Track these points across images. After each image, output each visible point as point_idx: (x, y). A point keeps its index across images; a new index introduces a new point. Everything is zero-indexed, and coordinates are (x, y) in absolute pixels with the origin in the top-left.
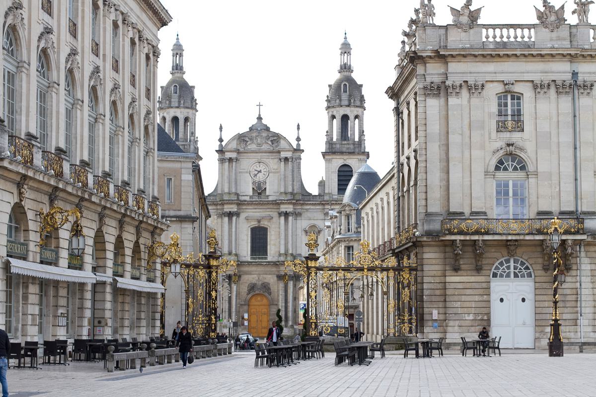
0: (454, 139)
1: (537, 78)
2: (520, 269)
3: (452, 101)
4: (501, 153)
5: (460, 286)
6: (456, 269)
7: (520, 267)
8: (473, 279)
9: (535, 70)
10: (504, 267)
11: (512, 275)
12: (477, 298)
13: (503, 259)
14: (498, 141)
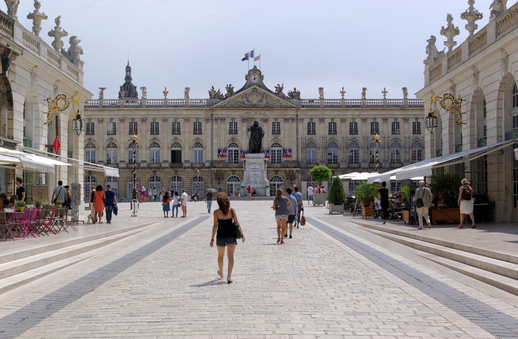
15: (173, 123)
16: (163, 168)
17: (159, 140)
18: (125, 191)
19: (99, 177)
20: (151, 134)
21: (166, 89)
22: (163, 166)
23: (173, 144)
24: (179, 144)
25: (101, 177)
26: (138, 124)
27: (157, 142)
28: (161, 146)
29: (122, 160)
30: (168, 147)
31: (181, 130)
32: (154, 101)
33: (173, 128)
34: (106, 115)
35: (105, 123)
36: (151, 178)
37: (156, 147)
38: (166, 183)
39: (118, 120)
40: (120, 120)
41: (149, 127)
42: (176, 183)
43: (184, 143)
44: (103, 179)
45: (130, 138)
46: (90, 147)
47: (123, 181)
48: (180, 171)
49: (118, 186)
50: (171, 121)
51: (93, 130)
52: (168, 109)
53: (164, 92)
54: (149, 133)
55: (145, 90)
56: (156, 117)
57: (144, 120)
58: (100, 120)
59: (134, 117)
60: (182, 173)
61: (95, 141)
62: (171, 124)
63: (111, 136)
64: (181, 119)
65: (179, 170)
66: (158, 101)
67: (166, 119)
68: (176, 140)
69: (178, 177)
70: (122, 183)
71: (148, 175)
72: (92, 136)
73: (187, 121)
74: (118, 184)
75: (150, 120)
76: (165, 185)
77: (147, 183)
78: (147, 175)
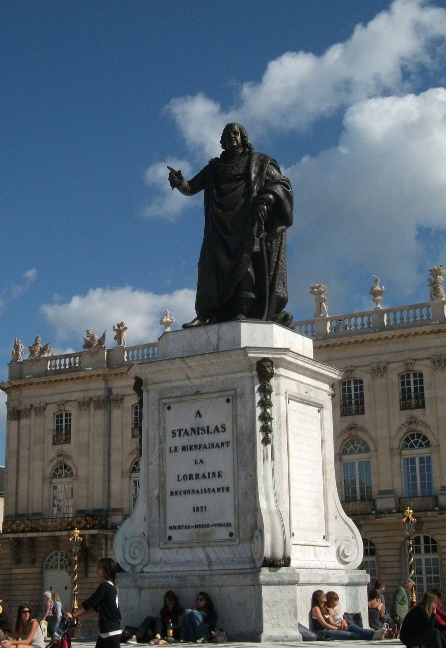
0: (24, 453)
1: (78, 396)
2: (65, 561)
3: (24, 422)
4: (55, 462)
5: (20, 577)
6: (18, 562)
7: (64, 559)
8: (29, 571)
9: (75, 391)
10: (54, 559)
11: (59, 566)
12: (31, 587)
13: (53, 553)
14: (52, 452)
15: (403, 377)
16: (380, 513)
17: (364, 430)
22: (378, 508)
23: (407, 440)
24: (425, 438)
27: (360, 434)
28: (372, 447)
30: (391, 450)
31: (427, 394)
33: (403, 390)
38: (391, 559)
42: (423, 557)
43: (435, 432)
48: (430, 522)
50: (396, 369)
52: (383, 337)
56: (355, 362)
60: (434, 525)
62: (396, 379)
64: (424, 362)
65: (426, 516)
66: (359, 320)
67: (382, 364)
68: (413, 426)
69: (427, 539)
73: (440, 365)
76: (388, 565)
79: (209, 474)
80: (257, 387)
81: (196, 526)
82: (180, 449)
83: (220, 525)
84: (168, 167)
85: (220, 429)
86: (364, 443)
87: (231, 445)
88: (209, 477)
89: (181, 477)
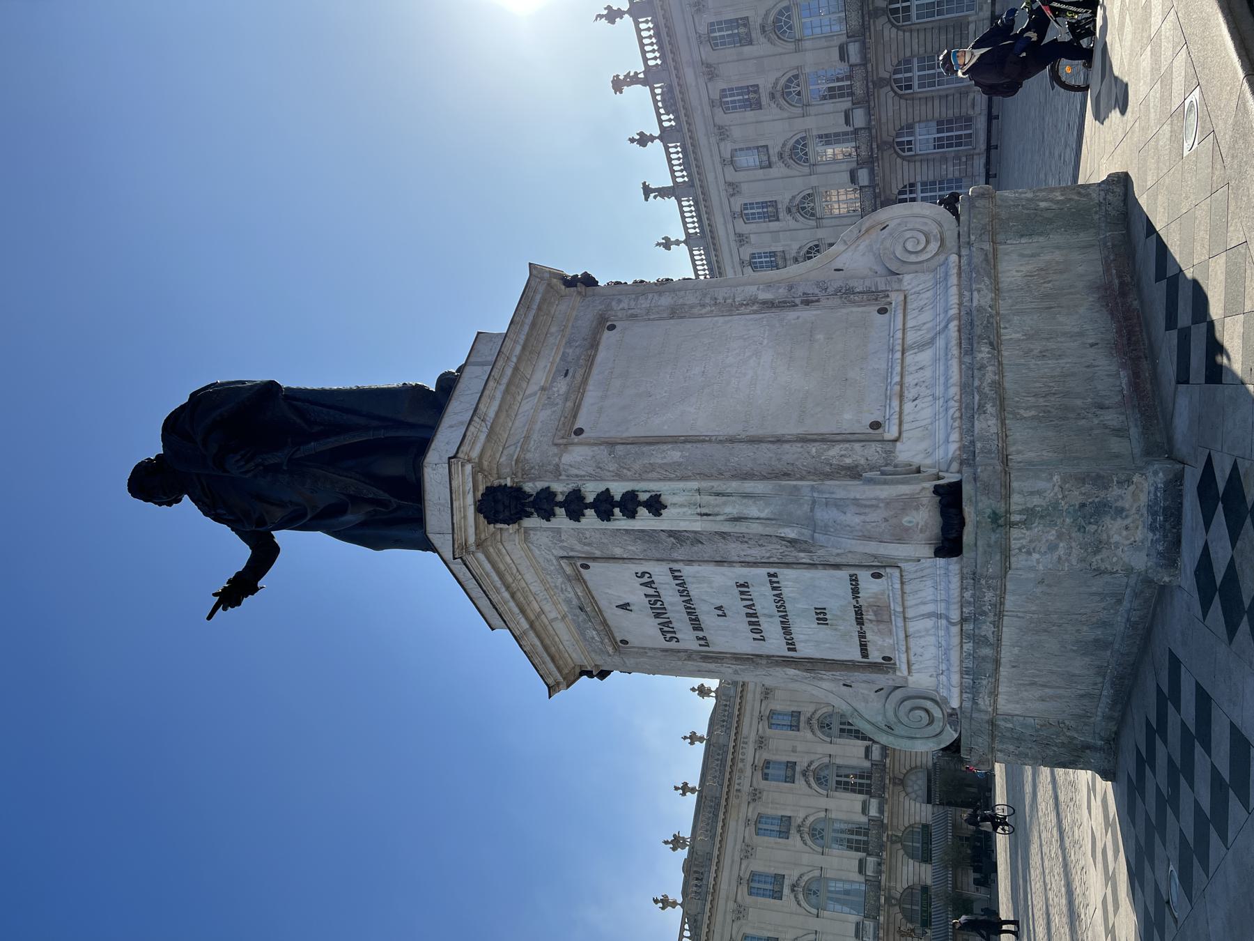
18: (944, 102)
19: (899, 177)
20: (751, 43)
21: (600, 16)
25: (899, 172)
26: (724, 86)
27: (771, 19)
29: (842, 120)
32: (649, 55)
34: (715, 177)
35: (740, 177)
36: (897, 19)
37: (789, 17)
39: (722, 145)
40: (722, 140)
41: (730, 52)
44: (906, 168)
45: (773, 105)
46: (812, 205)
47: (910, 110)
49: (927, 121)
51: (764, 204)
53: (612, 21)
54: (747, 49)
55: (621, 77)
57: (711, 72)
58: (731, 191)
59: (705, 100)
61: (794, 197)
63: (774, 159)
70: (917, 112)
71: (886, 33)
72: (782, 208)
74: (920, 122)
75: (707, 53)
77: (915, 34)
78: (887, 38)
79: (742, 599)
80: (544, 523)
81: (860, 621)
82: (701, 634)
83: (855, 591)
84: (209, 618)
85: (646, 579)
86: (780, 13)
87: (676, 566)
88: (752, 600)
89: (757, 636)
